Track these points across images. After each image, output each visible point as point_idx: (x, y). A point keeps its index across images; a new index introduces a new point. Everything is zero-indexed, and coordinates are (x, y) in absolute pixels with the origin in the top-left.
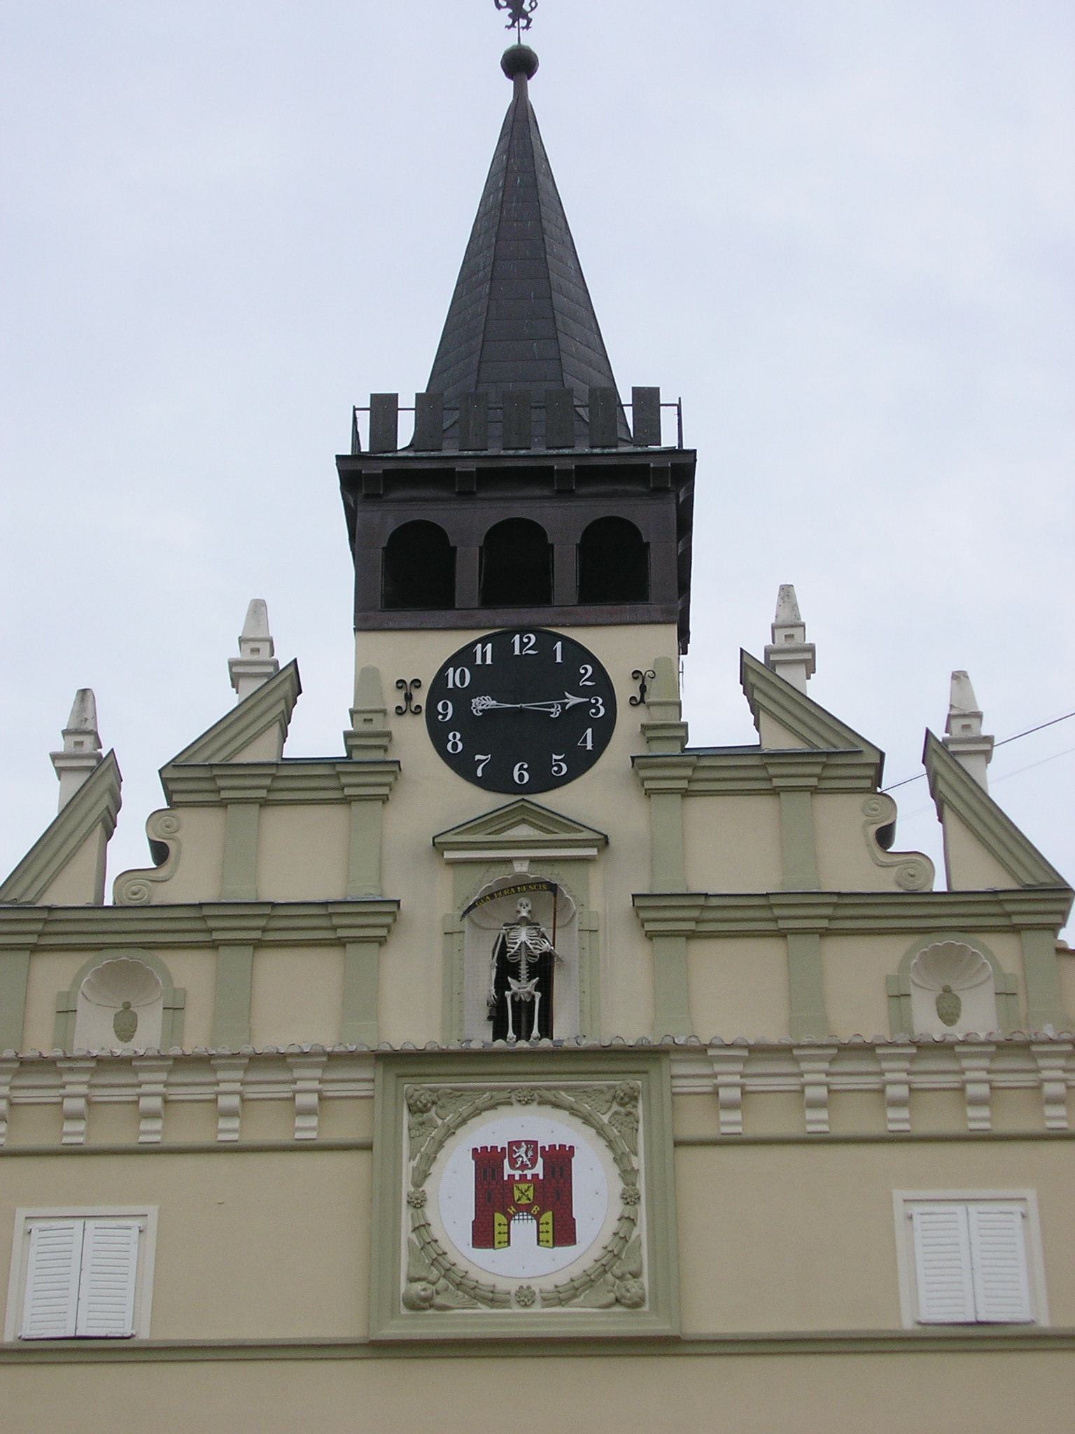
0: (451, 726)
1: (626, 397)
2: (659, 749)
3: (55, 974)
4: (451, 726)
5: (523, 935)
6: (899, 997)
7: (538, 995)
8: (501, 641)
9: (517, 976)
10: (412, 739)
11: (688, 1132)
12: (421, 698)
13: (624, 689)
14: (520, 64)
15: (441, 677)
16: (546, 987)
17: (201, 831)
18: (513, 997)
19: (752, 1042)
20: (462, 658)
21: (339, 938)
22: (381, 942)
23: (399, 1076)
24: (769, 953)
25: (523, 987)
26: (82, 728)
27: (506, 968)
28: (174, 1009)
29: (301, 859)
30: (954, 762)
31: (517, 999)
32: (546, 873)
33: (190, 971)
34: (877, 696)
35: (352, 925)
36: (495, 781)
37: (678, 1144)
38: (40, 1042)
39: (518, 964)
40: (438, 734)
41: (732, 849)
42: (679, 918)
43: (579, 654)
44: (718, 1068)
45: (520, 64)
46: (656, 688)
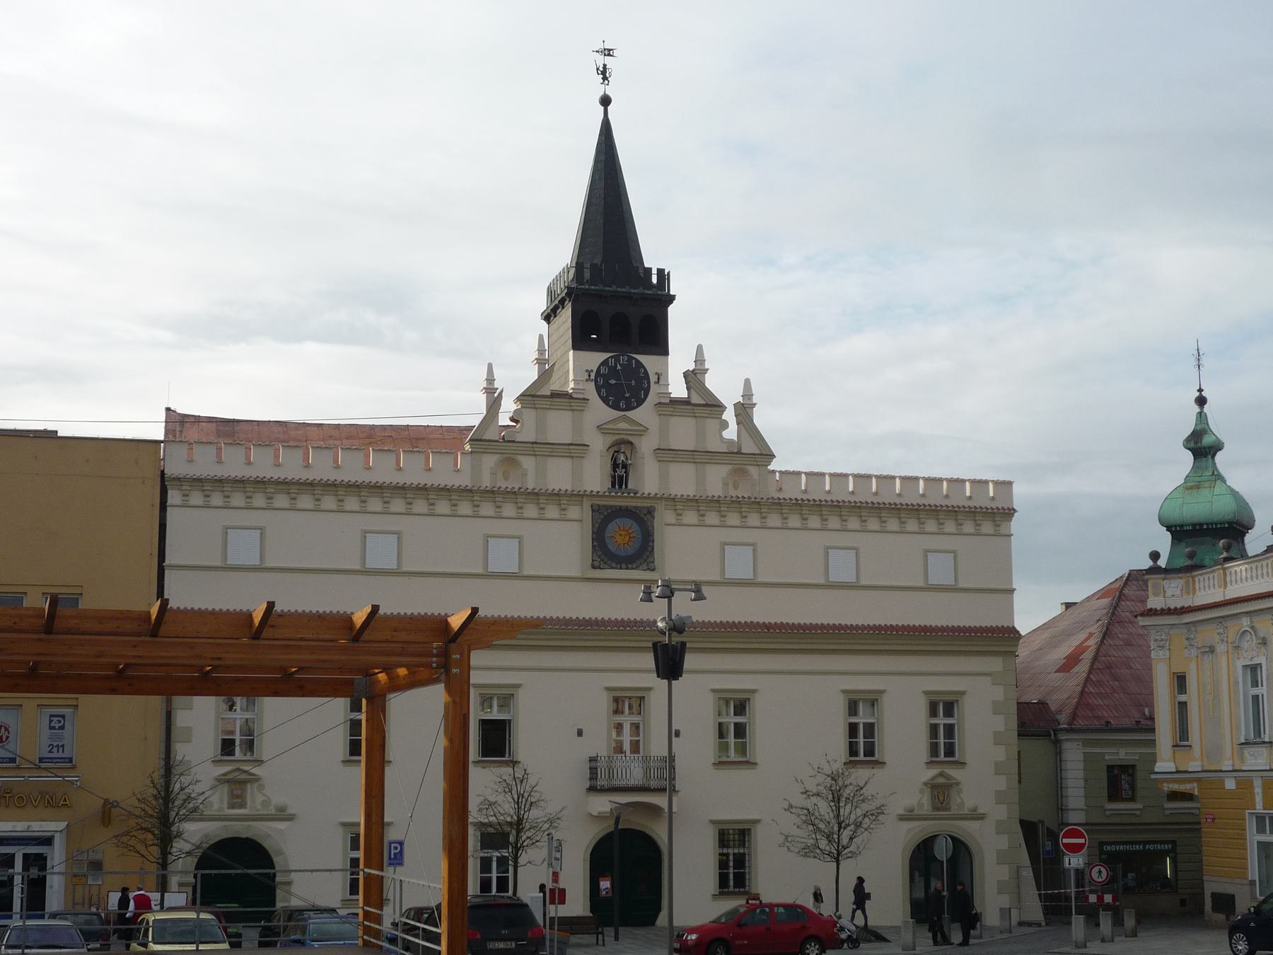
0: (602, 386)
1: (654, 271)
2: (663, 401)
3: (490, 461)
4: (602, 386)
5: (622, 457)
6: (726, 484)
8: (616, 358)
10: (591, 391)
12: (593, 376)
13: (653, 379)
14: (606, 101)
15: (599, 369)
17: (530, 416)
20: (605, 363)
24: (691, 467)
25: (621, 472)
26: (490, 379)
27: (615, 466)
28: (525, 475)
29: (559, 426)
30: (744, 410)
32: (630, 438)
33: (528, 463)
34: (723, 386)
35: (575, 450)
36: (615, 407)
38: (486, 483)
40: (598, 388)
41: (682, 433)
42: (666, 454)
43: (639, 364)
45: (606, 101)
46: (661, 377)
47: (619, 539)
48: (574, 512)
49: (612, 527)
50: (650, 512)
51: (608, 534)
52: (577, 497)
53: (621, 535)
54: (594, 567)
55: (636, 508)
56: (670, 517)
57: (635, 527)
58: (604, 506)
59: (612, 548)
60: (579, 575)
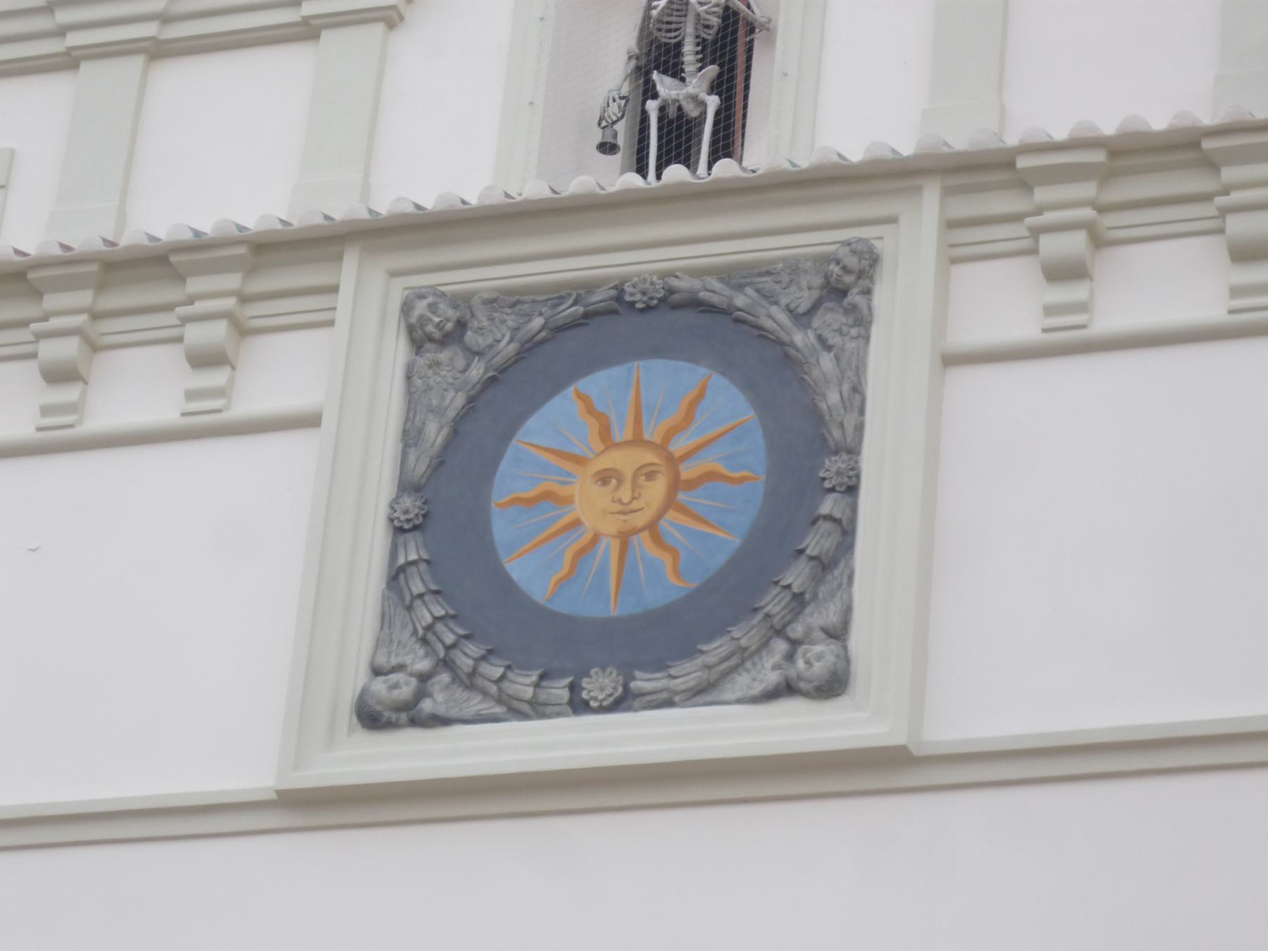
7: (713, 102)
9: (676, 72)
11: (973, 332)
16: (731, 86)
18: (662, 109)
19: (1109, 127)
21: (306, 21)
22: (391, 19)
23: (394, 274)
31: (672, 113)
37: (952, 360)
39: (679, 45)
44: (1043, 194)
47: (593, 507)
48: (285, 371)
49: (558, 421)
50: (844, 287)
51: (514, 477)
52: (288, 258)
53: (604, 487)
54: (371, 718)
55: (736, 275)
56: (1004, 301)
57: (727, 403)
58: (510, 300)
59: (533, 572)
60: (257, 776)
